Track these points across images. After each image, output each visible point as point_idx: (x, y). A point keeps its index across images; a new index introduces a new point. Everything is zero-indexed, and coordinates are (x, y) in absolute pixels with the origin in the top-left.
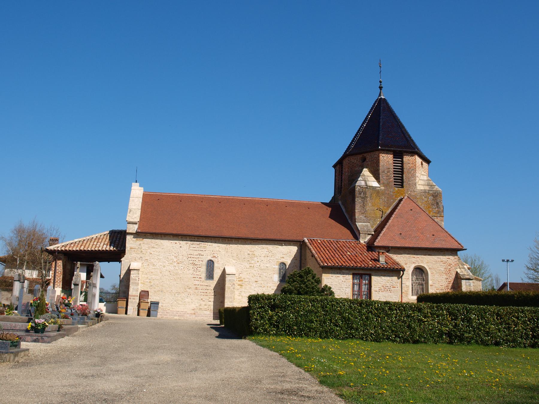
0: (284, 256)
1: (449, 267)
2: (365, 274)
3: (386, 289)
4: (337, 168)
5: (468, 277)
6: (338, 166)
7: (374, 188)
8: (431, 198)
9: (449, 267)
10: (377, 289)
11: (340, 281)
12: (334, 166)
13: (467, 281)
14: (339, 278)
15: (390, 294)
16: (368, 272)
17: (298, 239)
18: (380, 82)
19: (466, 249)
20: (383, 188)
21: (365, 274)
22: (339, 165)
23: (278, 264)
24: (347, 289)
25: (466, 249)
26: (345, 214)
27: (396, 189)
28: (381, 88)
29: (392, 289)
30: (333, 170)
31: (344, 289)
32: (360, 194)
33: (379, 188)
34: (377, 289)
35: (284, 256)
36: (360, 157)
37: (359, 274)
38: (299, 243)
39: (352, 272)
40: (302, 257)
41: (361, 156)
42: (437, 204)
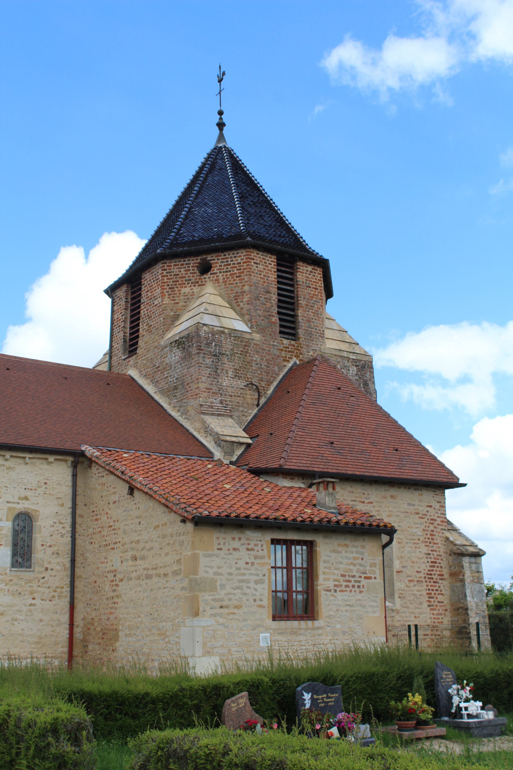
0: (28, 493)
1: (432, 527)
2: (299, 543)
3: (350, 583)
4: (121, 293)
5: (471, 549)
6: (124, 288)
7: (234, 333)
8: (353, 370)
9: (432, 527)
10: (331, 584)
11: (241, 564)
12: (111, 291)
13: (473, 560)
14: (236, 554)
15: (359, 596)
16: (308, 537)
17: (68, 446)
18: (221, 113)
19: (464, 485)
20: (257, 337)
21: (299, 543)
23: (12, 517)
24: (259, 587)
25: (464, 485)
26: (157, 397)
27: (285, 342)
28: (221, 125)
29: (364, 582)
31: (252, 585)
32: (208, 344)
33: (248, 336)
34: (331, 584)
35: (28, 493)
36: (194, 262)
37: (285, 542)
38: (70, 459)
39: (268, 536)
40: (78, 498)
41: (198, 259)
42: (366, 384)
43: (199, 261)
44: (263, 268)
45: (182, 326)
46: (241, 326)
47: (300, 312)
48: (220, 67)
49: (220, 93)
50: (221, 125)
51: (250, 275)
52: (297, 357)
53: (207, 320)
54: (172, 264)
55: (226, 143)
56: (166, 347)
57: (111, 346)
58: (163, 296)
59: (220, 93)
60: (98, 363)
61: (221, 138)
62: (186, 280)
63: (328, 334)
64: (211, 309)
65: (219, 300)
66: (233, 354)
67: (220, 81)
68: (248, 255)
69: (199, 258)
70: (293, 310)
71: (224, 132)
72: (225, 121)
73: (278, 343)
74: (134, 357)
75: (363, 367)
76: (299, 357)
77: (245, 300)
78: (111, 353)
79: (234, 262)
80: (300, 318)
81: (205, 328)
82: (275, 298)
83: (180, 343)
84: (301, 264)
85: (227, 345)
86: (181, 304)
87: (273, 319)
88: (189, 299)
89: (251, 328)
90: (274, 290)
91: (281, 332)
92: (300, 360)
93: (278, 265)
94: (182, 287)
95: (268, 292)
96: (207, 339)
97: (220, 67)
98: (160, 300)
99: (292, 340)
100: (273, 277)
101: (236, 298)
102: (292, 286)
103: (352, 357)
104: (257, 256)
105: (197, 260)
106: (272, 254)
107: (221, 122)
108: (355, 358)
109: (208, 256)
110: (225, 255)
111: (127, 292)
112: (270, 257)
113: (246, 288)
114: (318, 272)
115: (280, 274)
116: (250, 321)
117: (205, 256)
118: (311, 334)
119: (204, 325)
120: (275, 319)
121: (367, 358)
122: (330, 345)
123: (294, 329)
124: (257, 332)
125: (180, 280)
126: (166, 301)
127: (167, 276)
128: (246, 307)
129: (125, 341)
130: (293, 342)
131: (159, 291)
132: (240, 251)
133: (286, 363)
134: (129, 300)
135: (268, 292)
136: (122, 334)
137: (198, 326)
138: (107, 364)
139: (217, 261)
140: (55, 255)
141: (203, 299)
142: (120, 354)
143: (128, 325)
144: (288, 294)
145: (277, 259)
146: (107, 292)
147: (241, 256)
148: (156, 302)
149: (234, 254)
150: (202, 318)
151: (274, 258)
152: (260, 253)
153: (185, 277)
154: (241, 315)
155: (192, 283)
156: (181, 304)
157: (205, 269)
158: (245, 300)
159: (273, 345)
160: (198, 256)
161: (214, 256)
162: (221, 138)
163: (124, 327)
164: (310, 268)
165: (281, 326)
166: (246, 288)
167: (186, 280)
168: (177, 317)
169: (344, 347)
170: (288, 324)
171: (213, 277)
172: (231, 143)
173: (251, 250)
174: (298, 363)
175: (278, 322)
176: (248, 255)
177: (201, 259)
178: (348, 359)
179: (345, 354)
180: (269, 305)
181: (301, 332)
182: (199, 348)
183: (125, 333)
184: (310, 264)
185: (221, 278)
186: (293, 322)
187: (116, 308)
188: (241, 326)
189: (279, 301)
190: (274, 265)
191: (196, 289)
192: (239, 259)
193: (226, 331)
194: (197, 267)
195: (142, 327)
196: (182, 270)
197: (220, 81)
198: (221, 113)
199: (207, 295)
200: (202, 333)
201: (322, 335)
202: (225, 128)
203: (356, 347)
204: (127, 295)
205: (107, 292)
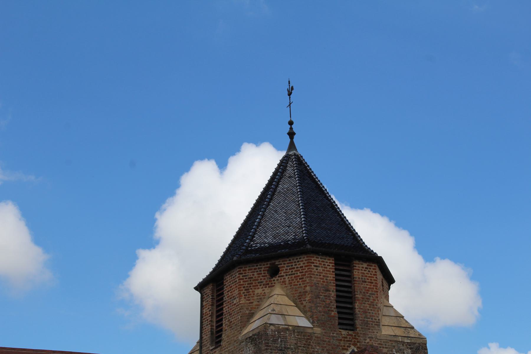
4: (208, 290)
6: (210, 287)
7: (298, 329)
12: (200, 288)
18: (291, 123)
20: (318, 330)
22: (213, 286)
27: (344, 332)
28: (291, 134)
30: (198, 295)
32: (275, 341)
33: (310, 331)
36: (264, 267)
41: (268, 265)
43: (269, 265)
44: (323, 269)
45: (254, 325)
46: (303, 322)
47: (357, 305)
48: (289, 82)
49: (290, 105)
50: (291, 134)
51: (311, 277)
52: (355, 345)
53: (274, 320)
54: (247, 269)
55: (296, 150)
56: (243, 342)
57: (201, 337)
58: (240, 296)
59: (290, 105)
60: (192, 350)
61: (292, 146)
62: (258, 283)
63: (385, 321)
64: (277, 309)
65: (286, 300)
66: (297, 348)
67: (290, 94)
68: (309, 260)
69: (269, 263)
70: (351, 303)
71: (294, 140)
72: (295, 130)
73: (337, 334)
74: (219, 348)
75: (418, 349)
76: (357, 344)
77: (307, 299)
78: (201, 342)
79: (297, 266)
80: (357, 311)
81: (272, 327)
82: (333, 294)
83: (255, 339)
84: (357, 262)
85: (292, 340)
86: (255, 303)
87: (333, 314)
88: (261, 299)
89: (312, 323)
90: (332, 287)
91: (340, 324)
92: (358, 348)
93: (336, 264)
94: (256, 289)
95: (328, 290)
96: (273, 336)
97: (289, 82)
98: (238, 299)
99: (350, 330)
100: (331, 276)
101: (300, 297)
102: (349, 282)
103: (406, 341)
104: (316, 260)
105: (267, 264)
106: (330, 256)
107: (291, 131)
108: (409, 341)
109: (276, 261)
110: (290, 260)
111: (213, 290)
112: (328, 260)
113: (308, 288)
114: (375, 269)
115: (338, 272)
116: (312, 317)
117: (273, 262)
118: (367, 324)
119: (271, 324)
120: (334, 313)
121: (421, 341)
122: (386, 331)
123: (352, 320)
124: (318, 327)
125: (254, 282)
126: (243, 301)
127: (243, 279)
128: (308, 305)
129: (212, 333)
130: (350, 332)
131: (236, 292)
132: (302, 257)
133: (344, 352)
134: (215, 297)
135: (328, 290)
136: (209, 327)
137: (266, 326)
138: (198, 352)
139: (284, 266)
140: (187, 168)
141: (271, 300)
142: (208, 346)
143: (215, 320)
144: (346, 289)
145: (335, 260)
146: (196, 288)
147: (302, 262)
148: (235, 302)
149: (297, 259)
150: (269, 319)
151: (332, 260)
152: (320, 257)
153: (258, 280)
154: (304, 312)
155: (264, 285)
156: (255, 303)
157: (274, 272)
158: (307, 299)
159: (333, 337)
160: (268, 261)
161: (281, 261)
162: (292, 146)
163: (211, 321)
164: (365, 265)
165: (339, 318)
166: (308, 288)
167: (258, 283)
168: (251, 315)
169: (399, 332)
170: (347, 317)
171: (281, 279)
172: (301, 151)
173: (312, 255)
174: (356, 350)
175: (337, 315)
176: (309, 260)
177: (270, 264)
178: (403, 343)
179: (400, 339)
180: (328, 301)
181: (358, 322)
182: (267, 345)
183: (212, 326)
184: (365, 262)
185: (287, 280)
186: (352, 314)
187: (204, 303)
188: (303, 322)
189: (338, 296)
190: (332, 266)
191: (267, 290)
192: (302, 263)
193: (290, 328)
194: (268, 270)
195: (225, 322)
196: (255, 273)
197: (290, 94)
198: (291, 123)
199: (275, 296)
200: (269, 332)
201: (378, 324)
202: (295, 136)
203: (411, 331)
204: (213, 293)
205: (196, 288)
